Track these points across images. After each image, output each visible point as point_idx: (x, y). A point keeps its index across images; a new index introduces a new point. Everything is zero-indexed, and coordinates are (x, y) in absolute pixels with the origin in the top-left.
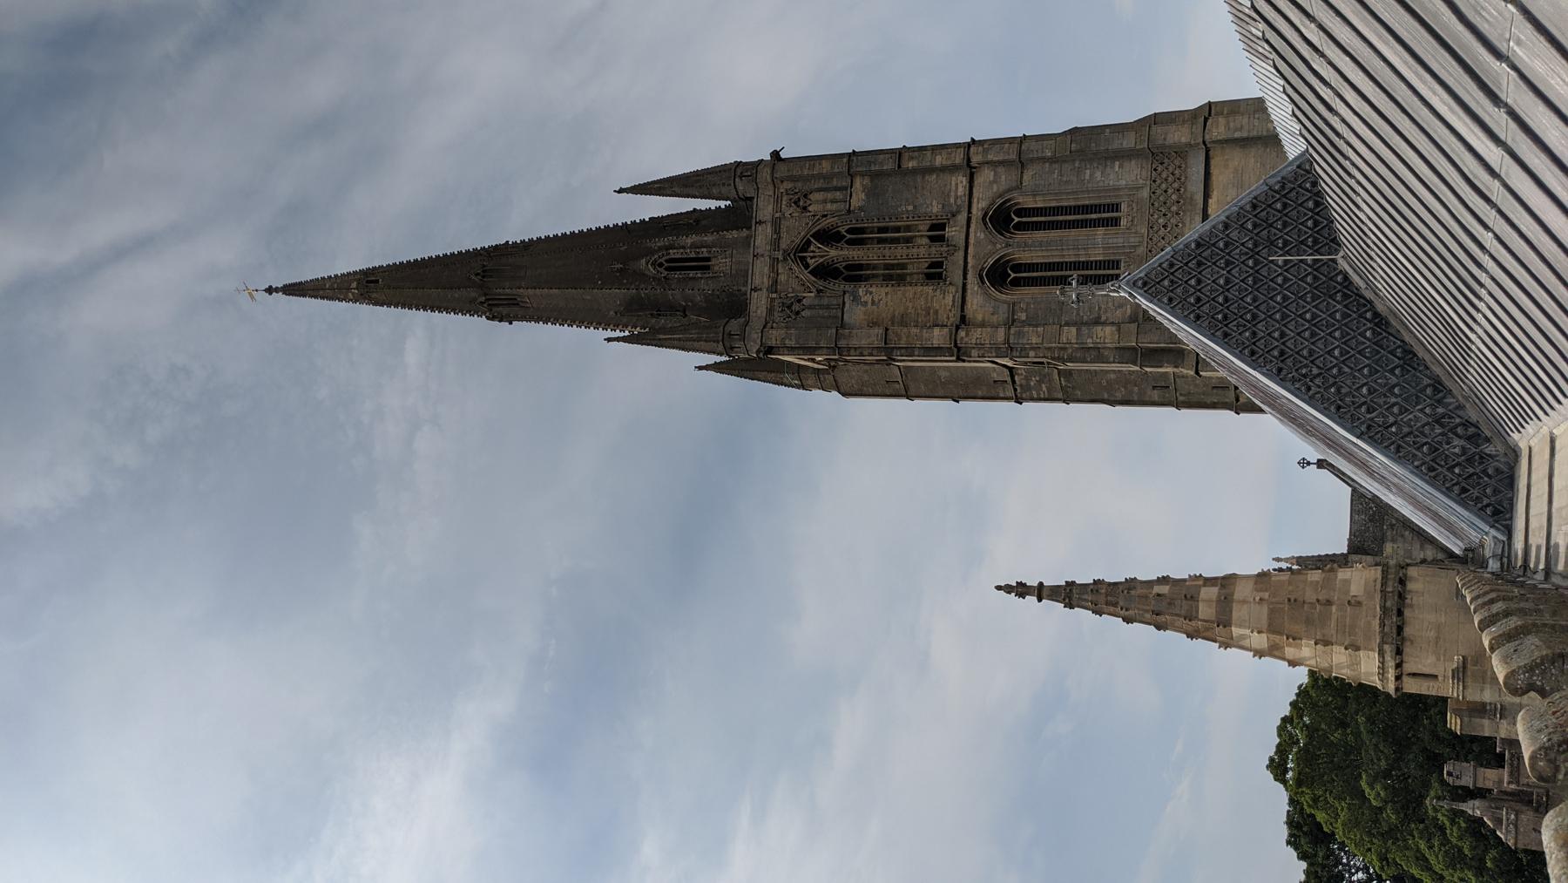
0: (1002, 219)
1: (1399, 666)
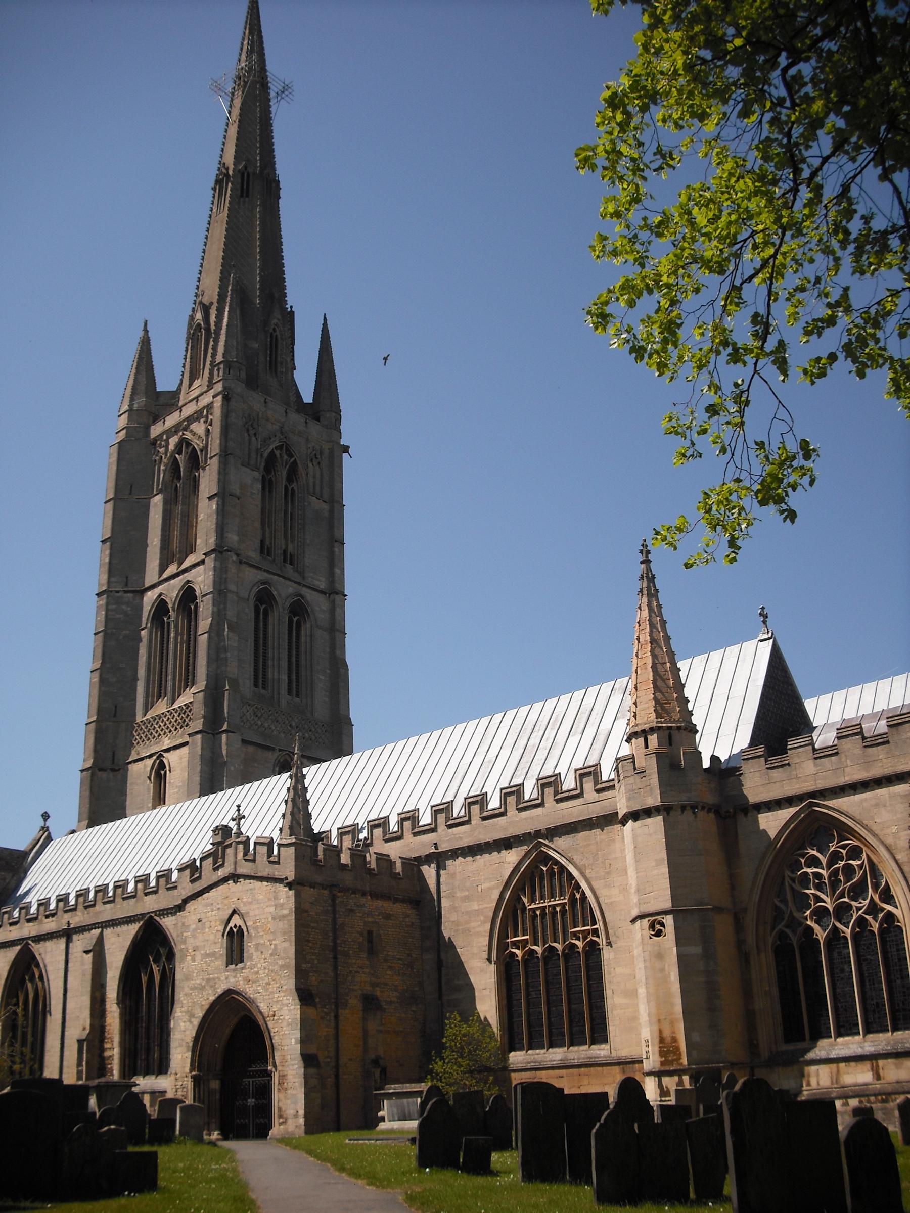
0: (299, 610)
1: (679, 728)
